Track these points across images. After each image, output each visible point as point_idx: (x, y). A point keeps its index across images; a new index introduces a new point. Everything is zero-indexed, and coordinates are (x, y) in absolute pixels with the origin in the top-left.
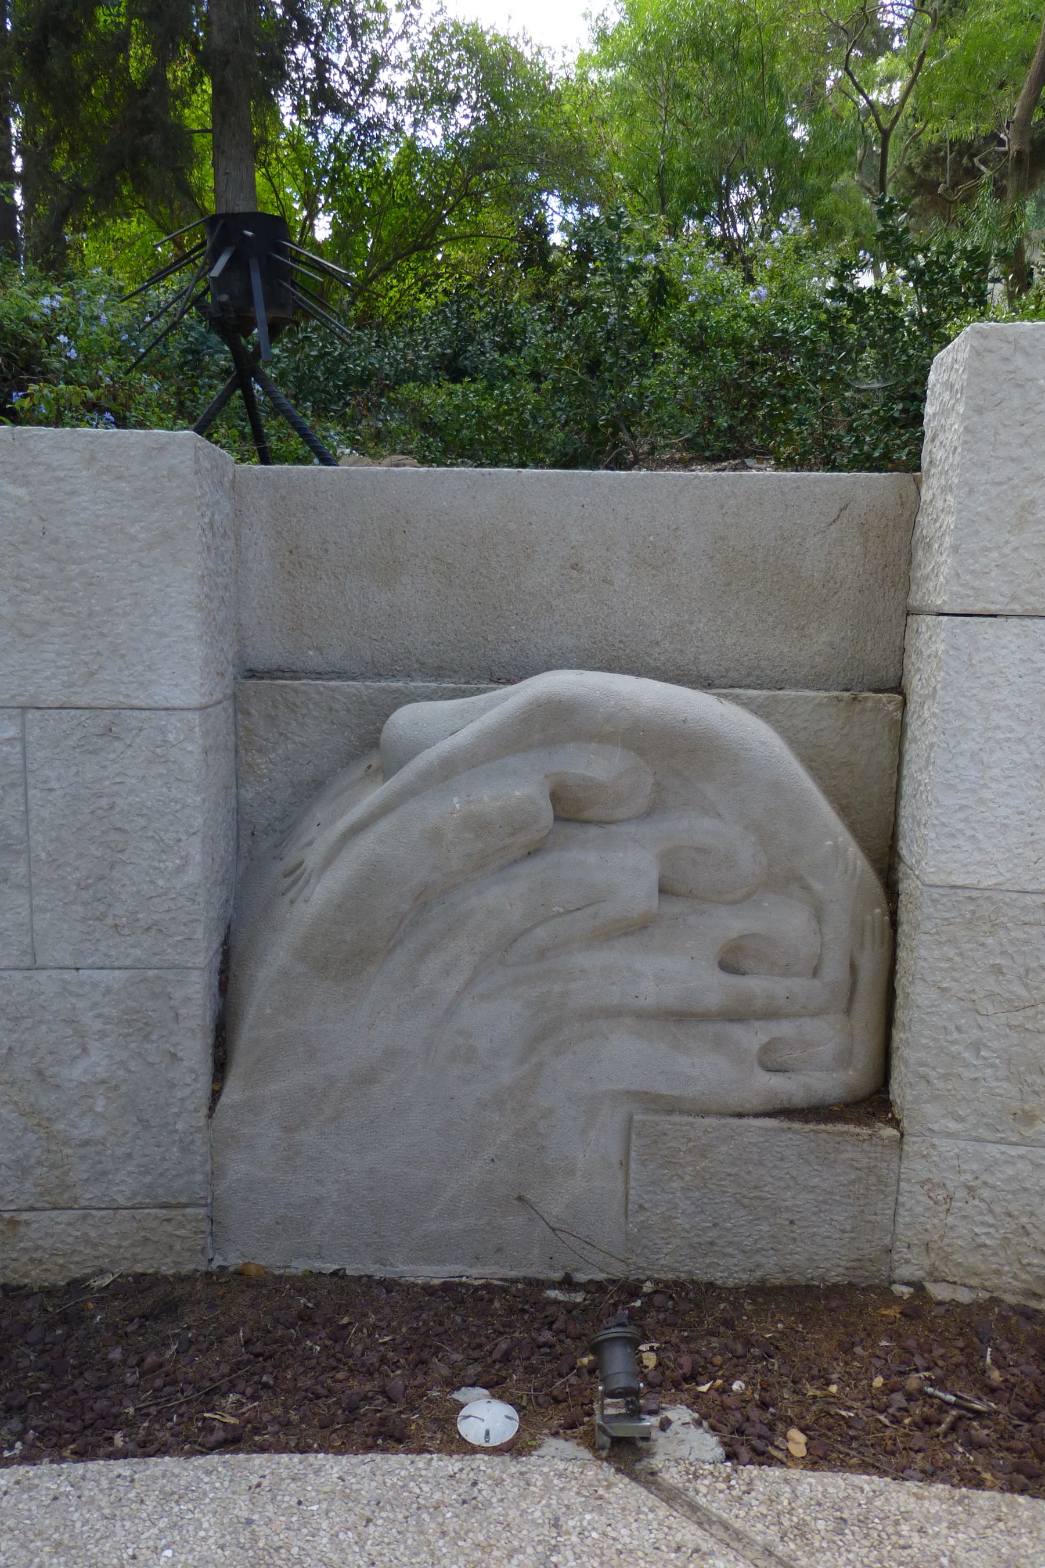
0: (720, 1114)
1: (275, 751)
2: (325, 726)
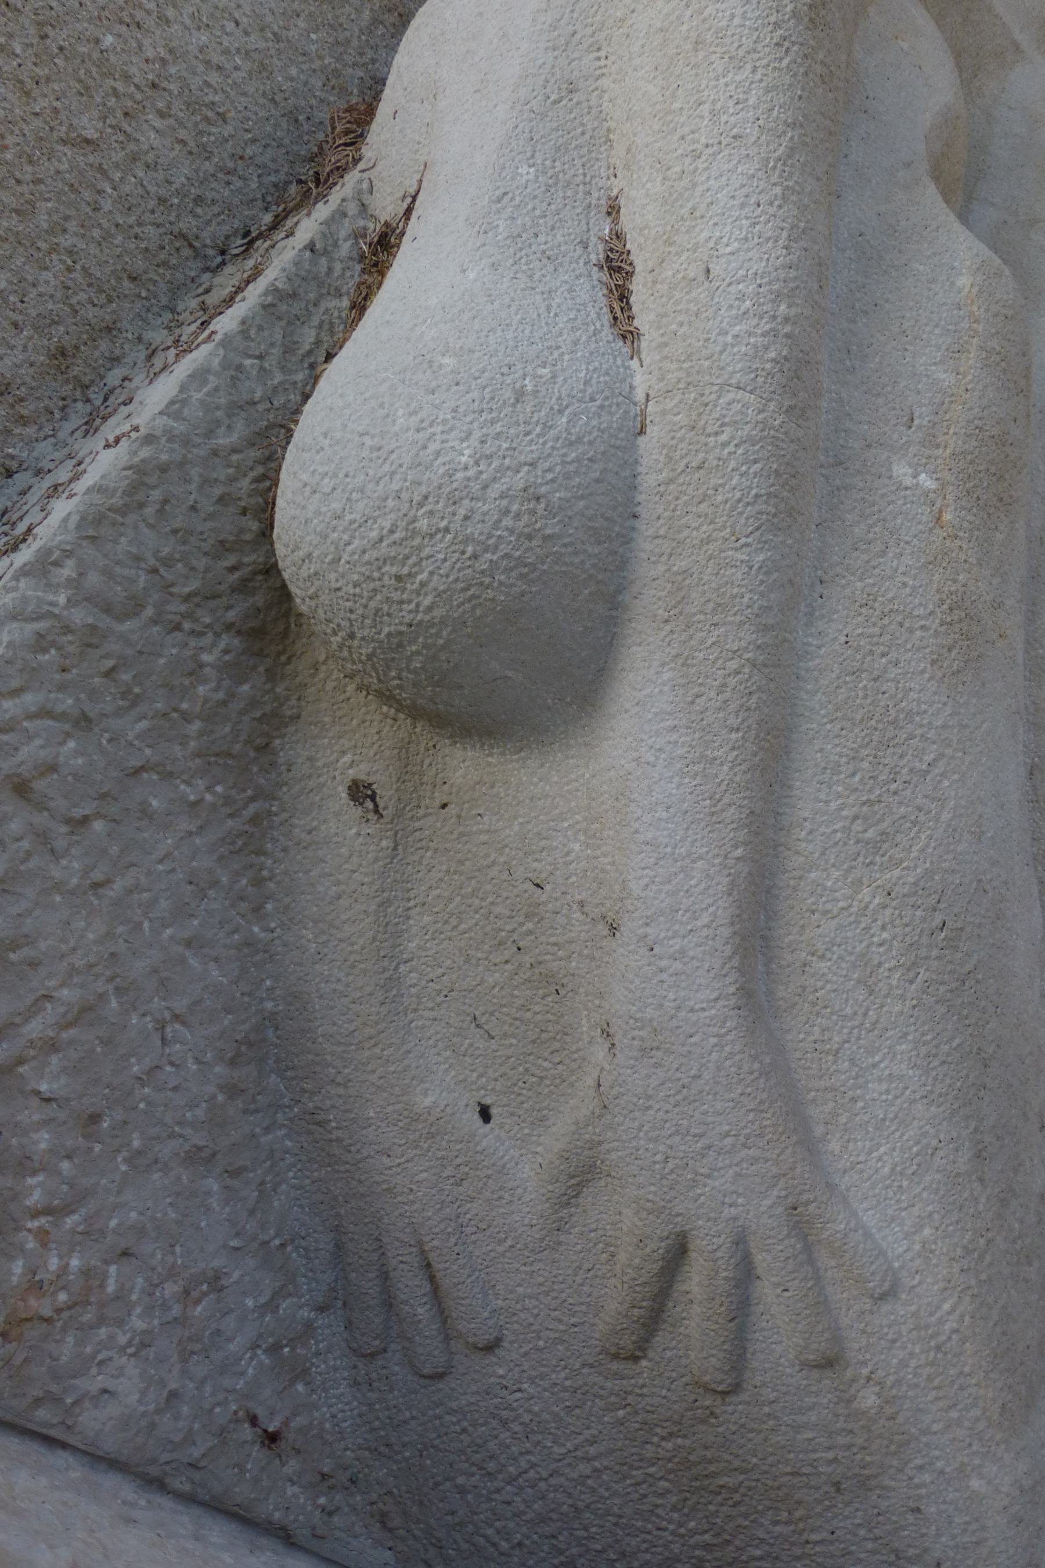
2: (70, 869)
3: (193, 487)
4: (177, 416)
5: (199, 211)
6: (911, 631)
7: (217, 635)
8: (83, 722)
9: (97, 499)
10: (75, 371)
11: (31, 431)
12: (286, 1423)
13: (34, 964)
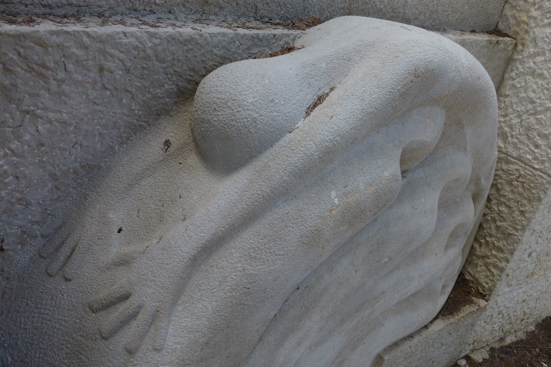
0: (419, 332)
1: (19, 138)
2: (93, 94)
3: (200, 53)
4: (211, 37)
5: (265, 6)
6: (303, 225)
7: (173, 84)
8: (128, 71)
9: (178, 35)
10: (205, 8)
11: (184, 9)
12: (8, 250)
13: (65, 103)
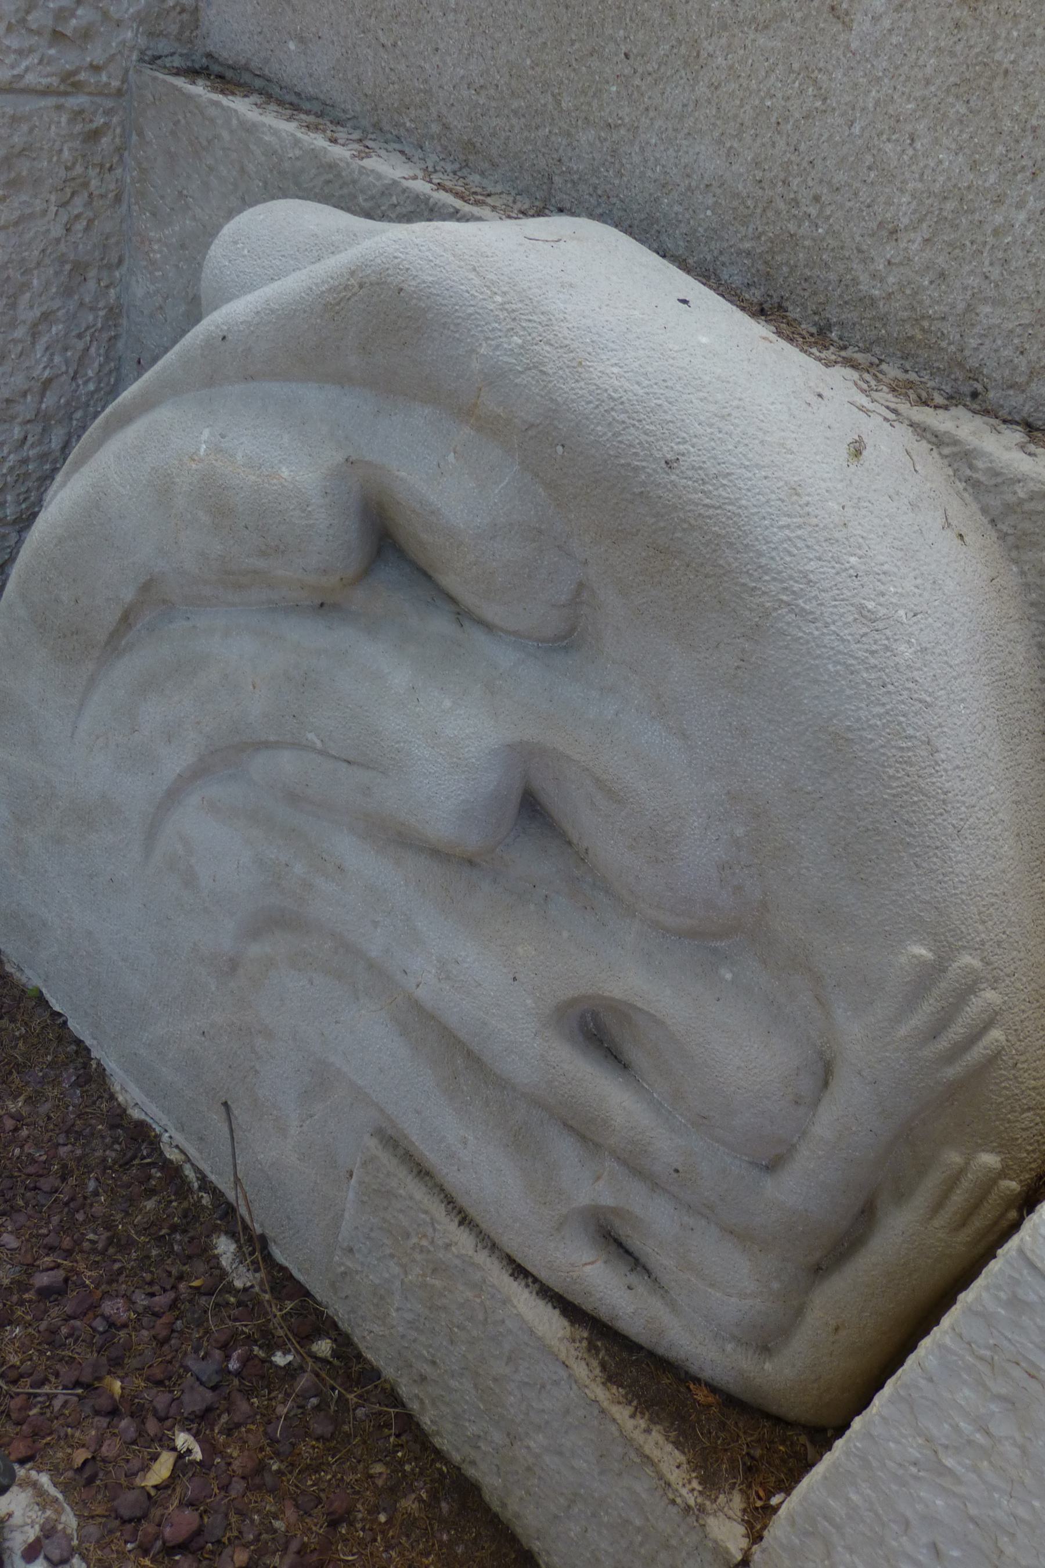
4: (361, 173)
5: (569, 185)
